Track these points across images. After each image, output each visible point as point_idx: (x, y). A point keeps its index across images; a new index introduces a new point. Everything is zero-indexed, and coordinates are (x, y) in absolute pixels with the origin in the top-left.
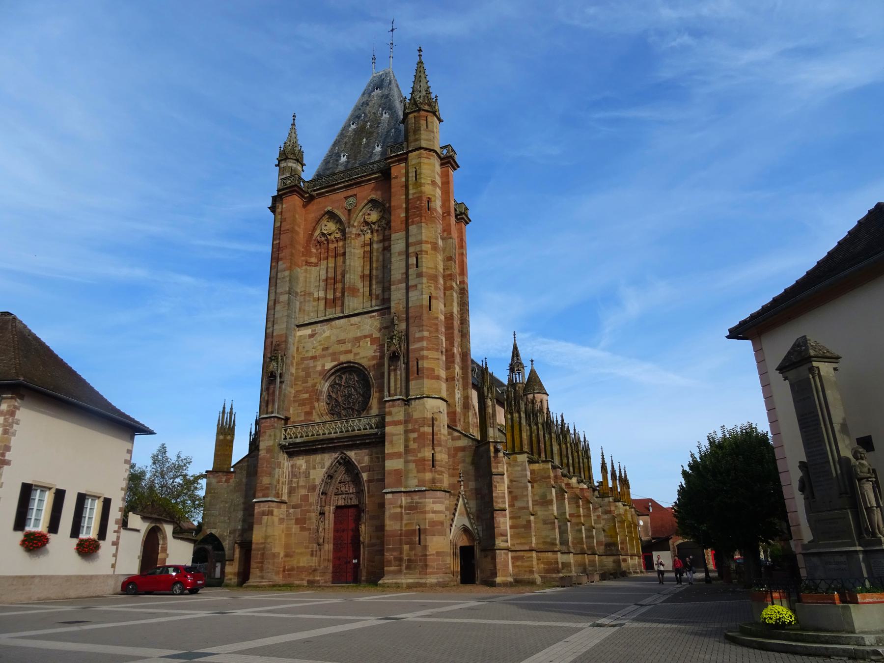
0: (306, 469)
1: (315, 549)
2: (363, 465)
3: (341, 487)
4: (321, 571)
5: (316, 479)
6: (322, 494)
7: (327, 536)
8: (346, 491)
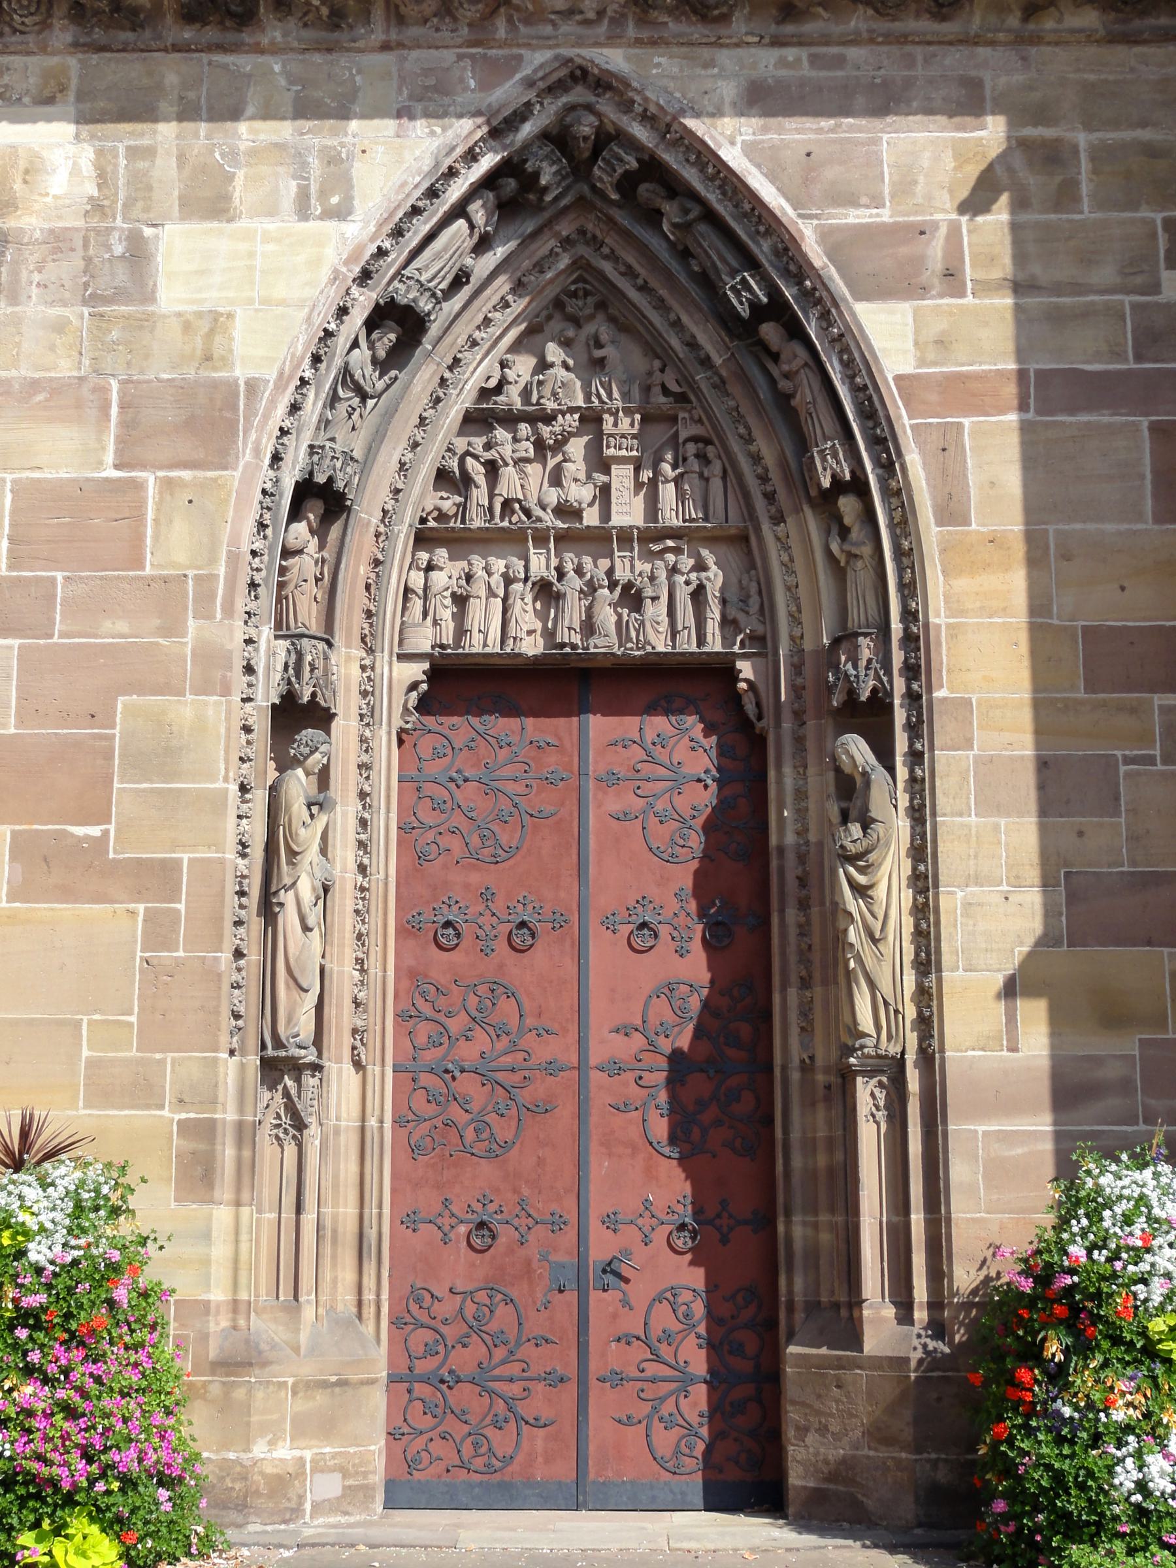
0: (97, 207)
1: (230, 1115)
2: (855, 217)
3: (492, 469)
4: (308, 1370)
5: (238, 330)
6: (305, 491)
7: (344, 972)
8: (565, 511)
